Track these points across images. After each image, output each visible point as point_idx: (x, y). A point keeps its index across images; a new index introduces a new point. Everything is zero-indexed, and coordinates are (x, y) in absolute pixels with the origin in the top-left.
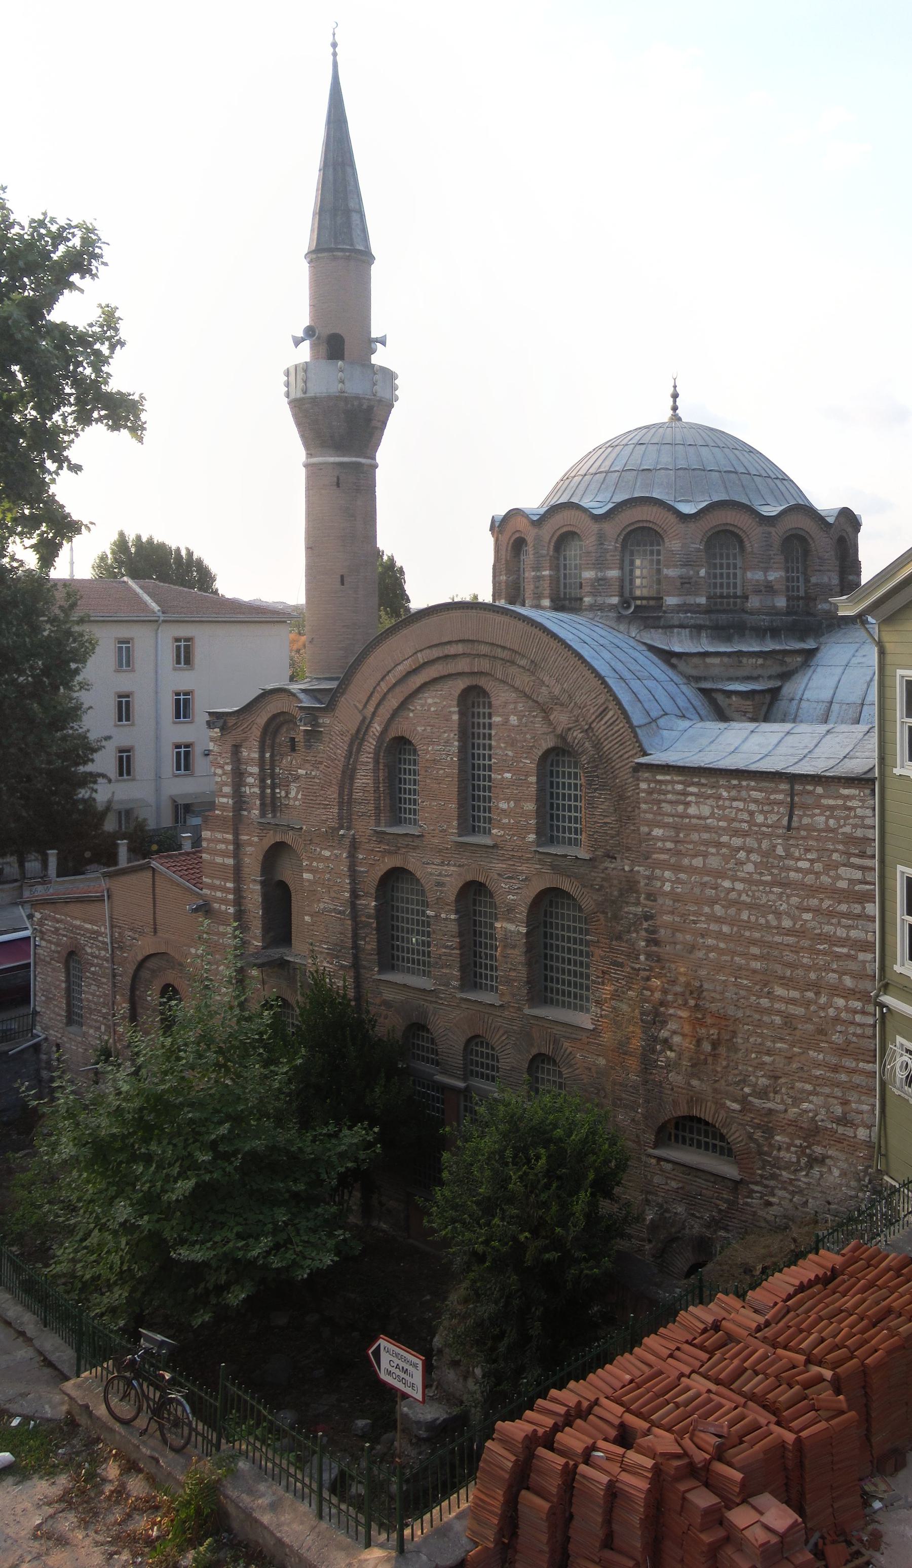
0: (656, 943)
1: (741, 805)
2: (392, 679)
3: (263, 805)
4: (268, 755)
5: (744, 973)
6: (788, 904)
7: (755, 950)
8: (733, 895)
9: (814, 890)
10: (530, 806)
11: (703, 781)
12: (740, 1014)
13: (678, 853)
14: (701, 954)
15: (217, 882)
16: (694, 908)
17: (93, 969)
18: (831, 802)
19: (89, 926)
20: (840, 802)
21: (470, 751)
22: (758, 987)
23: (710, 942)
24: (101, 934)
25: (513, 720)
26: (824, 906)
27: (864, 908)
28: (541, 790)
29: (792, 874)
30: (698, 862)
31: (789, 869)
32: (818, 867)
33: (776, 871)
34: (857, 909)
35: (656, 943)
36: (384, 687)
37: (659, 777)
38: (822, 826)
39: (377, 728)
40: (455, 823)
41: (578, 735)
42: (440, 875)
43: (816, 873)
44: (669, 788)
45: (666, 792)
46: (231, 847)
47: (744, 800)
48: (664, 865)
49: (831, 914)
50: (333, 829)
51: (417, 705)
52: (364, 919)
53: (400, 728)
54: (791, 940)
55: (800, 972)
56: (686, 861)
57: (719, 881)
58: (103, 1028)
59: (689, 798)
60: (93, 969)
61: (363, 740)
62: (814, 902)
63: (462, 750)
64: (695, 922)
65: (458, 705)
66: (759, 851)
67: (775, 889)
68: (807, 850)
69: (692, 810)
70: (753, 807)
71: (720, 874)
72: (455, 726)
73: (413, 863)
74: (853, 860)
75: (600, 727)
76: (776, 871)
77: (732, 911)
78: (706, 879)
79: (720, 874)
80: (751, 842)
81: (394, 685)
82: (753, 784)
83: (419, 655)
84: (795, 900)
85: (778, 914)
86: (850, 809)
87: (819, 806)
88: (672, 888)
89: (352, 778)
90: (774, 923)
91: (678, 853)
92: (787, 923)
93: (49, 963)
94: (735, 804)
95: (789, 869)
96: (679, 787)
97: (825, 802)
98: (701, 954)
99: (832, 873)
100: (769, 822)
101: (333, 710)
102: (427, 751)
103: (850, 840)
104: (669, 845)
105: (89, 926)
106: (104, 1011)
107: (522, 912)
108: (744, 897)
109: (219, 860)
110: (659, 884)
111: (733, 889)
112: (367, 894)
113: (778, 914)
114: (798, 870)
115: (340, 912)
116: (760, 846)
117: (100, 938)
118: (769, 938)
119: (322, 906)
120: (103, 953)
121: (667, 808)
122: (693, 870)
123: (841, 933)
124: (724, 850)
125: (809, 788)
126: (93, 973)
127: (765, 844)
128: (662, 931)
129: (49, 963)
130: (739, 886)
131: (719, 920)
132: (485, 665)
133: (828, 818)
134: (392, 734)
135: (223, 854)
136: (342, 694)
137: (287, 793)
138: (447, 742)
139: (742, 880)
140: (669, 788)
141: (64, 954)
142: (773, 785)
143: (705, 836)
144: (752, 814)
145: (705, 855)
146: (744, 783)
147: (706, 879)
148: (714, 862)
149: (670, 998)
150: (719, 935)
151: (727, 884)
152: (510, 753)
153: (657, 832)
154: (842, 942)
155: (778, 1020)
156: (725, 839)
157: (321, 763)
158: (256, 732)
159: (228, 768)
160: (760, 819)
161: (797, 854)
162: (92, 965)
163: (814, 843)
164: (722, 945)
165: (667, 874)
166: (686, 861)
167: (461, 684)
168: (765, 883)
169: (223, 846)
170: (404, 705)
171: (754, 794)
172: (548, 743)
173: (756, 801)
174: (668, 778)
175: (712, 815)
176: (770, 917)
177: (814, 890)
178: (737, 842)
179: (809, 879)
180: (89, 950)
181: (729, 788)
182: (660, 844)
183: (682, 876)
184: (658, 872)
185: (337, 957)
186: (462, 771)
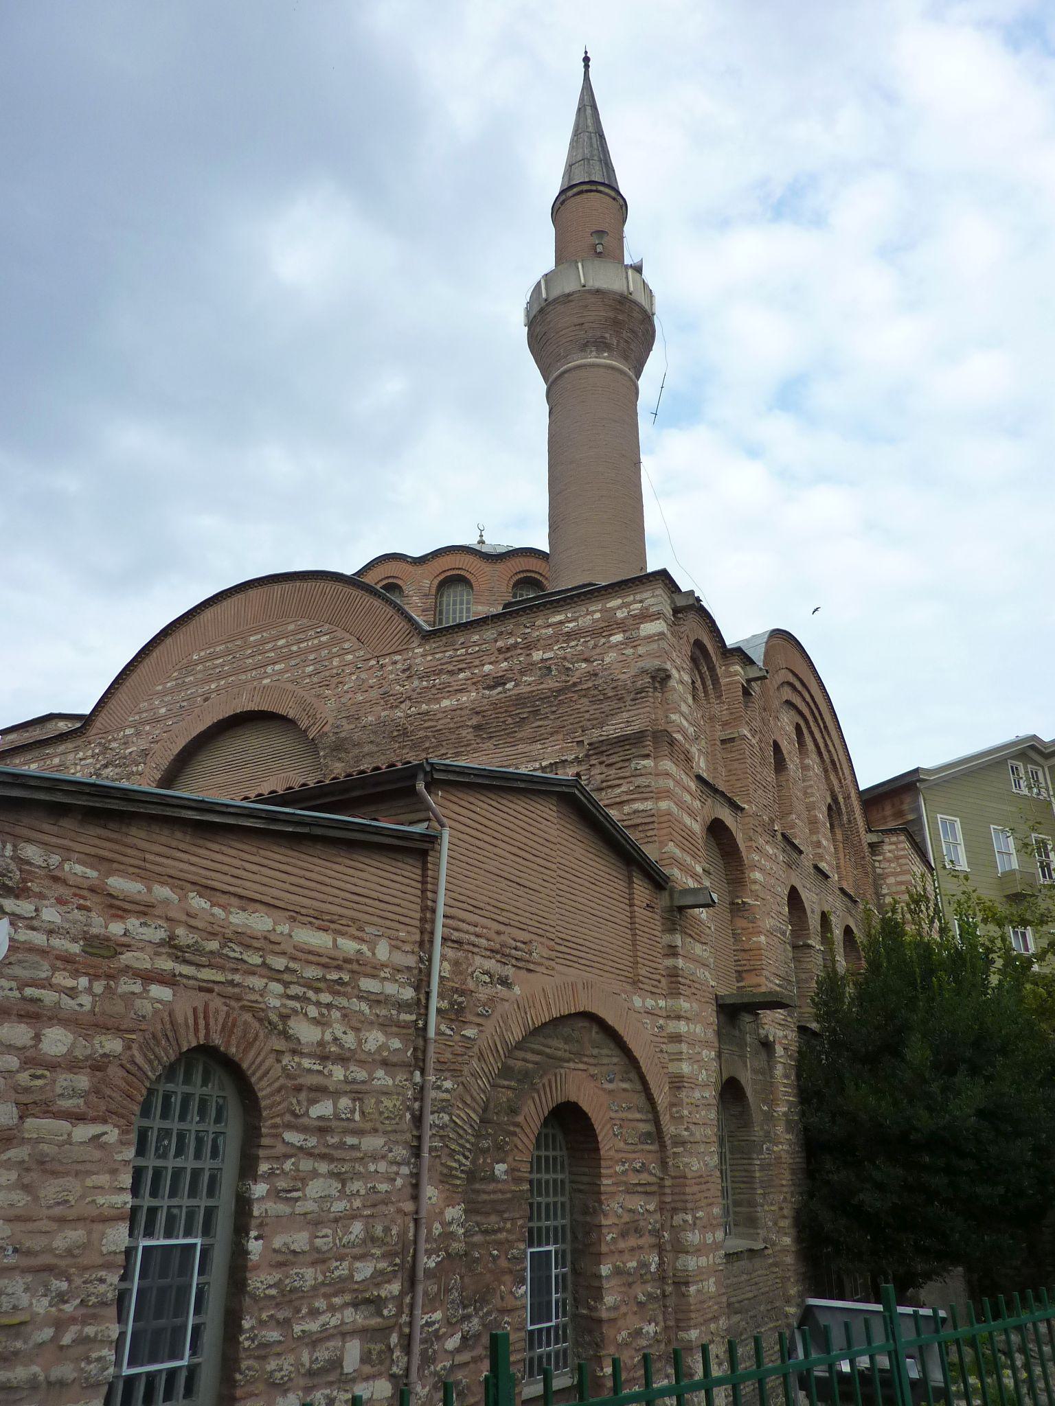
24: (374, 970)
58: (352, 1353)
106: (364, 1270)
109: (688, 820)
117: (367, 984)
120: (375, 1039)
126: (322, 1129)
162: (320, 1091)
180: (307, 1033)
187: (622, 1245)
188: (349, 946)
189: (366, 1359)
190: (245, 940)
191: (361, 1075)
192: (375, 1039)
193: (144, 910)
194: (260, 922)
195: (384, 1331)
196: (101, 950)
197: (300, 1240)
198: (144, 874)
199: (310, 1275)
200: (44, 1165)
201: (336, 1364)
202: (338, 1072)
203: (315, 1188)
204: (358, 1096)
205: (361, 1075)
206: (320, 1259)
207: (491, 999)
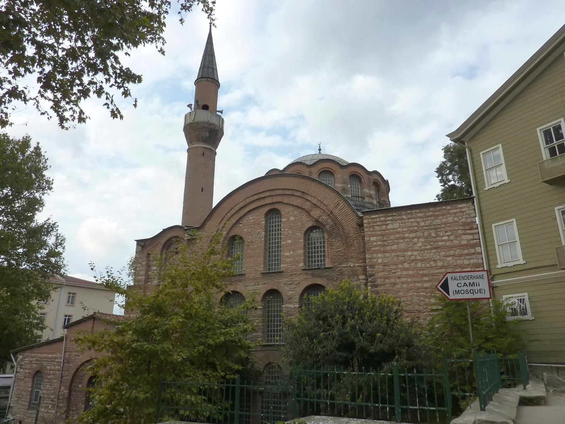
0: (376, 286)
1: (413, 220)
2: (233, 211)
5: (421, 290)
6: (440, 255)
7: (426, 279)
8: (413, 258)
9: (451, 248)
10: (301, 252)
11: (394, 214)
12: (421, 308)
13: (384, 245)
14: (399, 286)
17: (49, 377)
18: (455, 211)
19: (50, 356)
20: (459, 210)
21: (268, 237)
22: (429, 295)
23: (403, 280)
25: (292, 218)
26: (457, 253)
27: (475, 250)
28: (305, 246)
29: (440, 243)
30: (395, 247)
32: (452, 238)
33: (432, 244)
34: (472, 251)
35: (376, 286)
36: (229, 215)
37: (372, 217)
38: (452, 221)
39: (224, 233)
40: (262, 266)
41: (325, 217)
43: (451, 240)
44: (378, 220)
47: (414, 218)
48: (378, 252)
49: (460, 256)
51: (245, 221)
53: (236, 231)
56: (388, 248)
57: (405, 253)
58: (50, 406)
59: (388, 222)
60: (49, 377)
62: (452, 252)
63: (266, 236)
64: (395, 273)
65: (265, 217)
67: (432, 251)
68: (446, 232)
69: (389, 227)
70: (419, 220)
72: (263, 227)
73: (239, 288)
74: (467, 232)
75: (336, 212)
76: (432, 244)
77: (413, 264)
78: (399, 253)
80: (419, 234)
81: (234, 214)
82: (418, 211)
83: (247, 200)
84: (443, 253)
85: (435, 261)
86: (463, 212)
87: (449, 214)
88: (383, 261)
91: (384, 245)
92: (440, 264)
93: (23, 380)
94: (410, 220)
96: (383, 218)
97: (451, 211)
98: (399, 286)
99: (458, 239)
100: (427, 224)
101: (203, 228)
102: (247, 239)
103: (465, 224)
104: (379, 243)
105: (50, 356)
106: (53, 397)
108: (418, 257)
110: (375, 260)
111: (412, 255)
113: (435, 261)
114: (442, 241)
116: (423, 235)
117: (57, 360)
118: (432, 272)
120: (57, 367)
121: (377, 228)
122: (393, 251)
123: (466, 262)
124: (407, 240)
125: (444, 207)
126: (49, 379)
127: (426, 234)
128: (379, 280)
129: (23, 380)
132: (279, 199)
133: (454, 217)
134: (231, 234)
136: (208, 221)
138: (259, 233)
140: (378, 220)
141: (33, 373)
142: (427, 210)
144: (418, 223)
146: (414, 211)
147: (399, 253)
148: (402, 246)
150: (407, 276)
151: (409, 253)
152: (290, 232)
153: (373, 239)
156: (406, 235)
158: (160, 247)
159: (144, 263)
160: (422, 224)
161: (442, 234)
163: (449, 229)
164: (409, 280)
165: (379, 255)
166: (388, 248)
168: (428, 249)
170: (238, 222)
171: (418, 215)
172: (310, 224)
173: (420, 217)
174: (377, 216)
175: (400, 227)
176: (432, 263)
177: (451, 248)
178: (412, 235)
179: (448, 244)
180: (48, 368)
181: (406, 215)
182: (375, 243)
183: (387, 255)
184: (375, 255)
186: (265, 245)
188: (54, 356)
189: (52, 407)
190: (43, 358)
191: (54, 372)
192: (57, 367)
193: (34, 357)
194: (44, 355)
195: (55, 405)
196: (31, 361)
197: (45, 392)
198: (35, 353)
199: (46, 396)
200: (25, 382)
201: (48, 407)
202: (52, 372)
203: (48, 386)
204: (54, 375)
205: (54, 372)
206: (48, 394)
207: (75, 359)
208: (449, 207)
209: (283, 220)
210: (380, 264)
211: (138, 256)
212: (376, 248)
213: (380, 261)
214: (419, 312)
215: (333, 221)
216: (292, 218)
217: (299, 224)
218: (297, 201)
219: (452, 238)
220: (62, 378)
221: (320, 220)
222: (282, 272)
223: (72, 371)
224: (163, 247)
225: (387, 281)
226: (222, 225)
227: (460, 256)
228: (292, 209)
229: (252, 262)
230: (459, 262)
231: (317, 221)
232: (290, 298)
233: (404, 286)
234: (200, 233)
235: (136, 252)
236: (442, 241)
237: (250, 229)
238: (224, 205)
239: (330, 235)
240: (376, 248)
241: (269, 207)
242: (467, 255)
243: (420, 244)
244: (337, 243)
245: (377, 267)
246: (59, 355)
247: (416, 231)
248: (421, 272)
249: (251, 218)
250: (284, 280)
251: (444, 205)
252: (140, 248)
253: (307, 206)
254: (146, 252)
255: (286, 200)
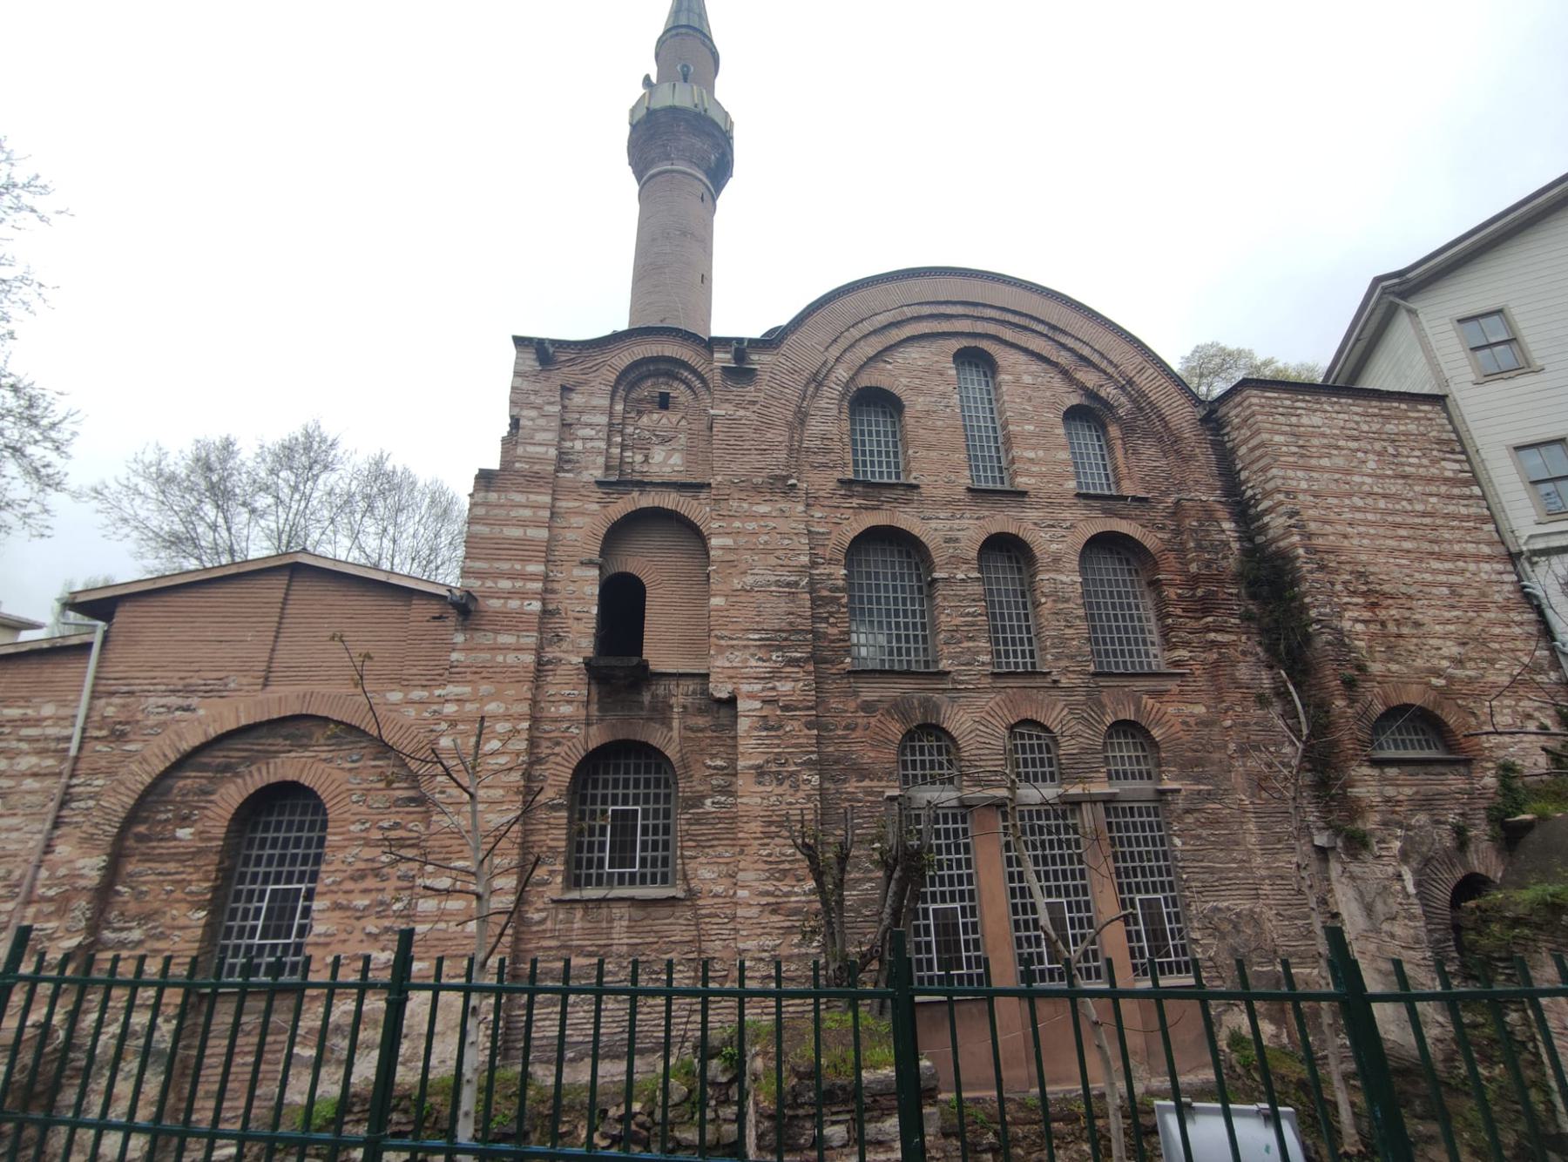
1: (1346, 417)
2: (867, 327)
3: (608, 468)
4: (619, 407)
8: (1366, 488)
10: (1064, 455)
12: (1411, 591)
13: (1302, 456)
14: (1356, 541)
15: (505, 566)
16: (1335, 501)
23: (1362, 529)
25: (1027, 379)
30: (1325, 462)
31: (1403, 464)
35: (1310, 536)
36: (855, 333)
39: (842, 373)
42: (951, 529)
45: (1276, 407)
46: (547, 514)
48: (1295, 466)
50: (777, 478)
52: (825, 593)
54: (1427, 520)
55: (1446, 546)
56: (1314, 462)
61: (820, 384)
66: (1375, 452)
70: (1357, 418)
71: (1348, 472)
73: (905, 519)
77: (1369, 501)
78: (1337, 476)
79: (1348, 472)
80: (1363, 444)
89: (802, 422)
90: (1409, 508)
91: (1302, 456)
92: (1419, 507)
95: (1403, 464)
96: (1288, 403)
101: (778, 347)
102: (915, 404)
107: (1073, 562)
108: (1376, 489)
110: (1295, 483)
112: (830, 562)
114: (1410, 465)
115: (788, 585)
119: (749, 580)
121: (1281, 419)
122: (1323, 469)
123: (1464, 511)
130: (1368, 480)
131: (1358, 509)
132: (992, 329)
134: (865, 381)
135: (523, 523)
137: (646, 457)
138: (943, 395)
139: (1369, 475)
143: (1325, 441)
144: (1357, 423)
145: (1329, 456)
147: (1337, 476)
148: (1340, 462)
149: (1339, 587)
151: (1357, 479)
153: (1278, 438)
154: (1468, 518)
155: (1445, 591)
156: (1342, 443)
157: (754, 403)
160: (1365, 427)
164: (1372, 531)
166: (1314, 462)
167: (956, 345)
168: (1388, 477)
169: (527, 513)
172: (1074, 399)
176: (1404, 503)
182: (1284, 449)
184: (1290, 473)
185: (779, 648)
187: (349, 885)
208: (1403, 406)
209: (1003, 377)
210: (1305, 491)
211: (525, 385)
212: (1291, 459)
213: (1304, 485)
214: (1410, 597)
215: (1134, 401)
216: (1027, 379)
217: (1048, 394)
218: (1036, 344)
219: (1425, 461)
220: (63, 804)
221: (1103, 394)
222: (1024, 494)
223: (139, 776)
224: (618, 381)
225: (1328, 529)
226: (835, 352)
227: (1450, 497)
228: (1022, 358)
229: (937, 461)
230: (1451, 509)
231: (1091, 394)
232: (1056, 560)
233: (1365, 542)
234: (766, 358)
235: (517, 374)
236: (1410, 465)
237: (917, 381)
238: (837, 305)
239: (1128, 429)
240: (1291, 459)
241: (965, 343)
242: (1461, 497)
243: (1371, 465)
244: (1149, 451)
245: (1301, 497)
246: (48, 710)
247: (1356, 439)
248: (1390, 519)
249: (915, 355)
250: (1033, 515)
251: (1396, 400)
252: (532, 363)
253: (1064, 358)
254: (558, 377)
255: (1008, 334)
